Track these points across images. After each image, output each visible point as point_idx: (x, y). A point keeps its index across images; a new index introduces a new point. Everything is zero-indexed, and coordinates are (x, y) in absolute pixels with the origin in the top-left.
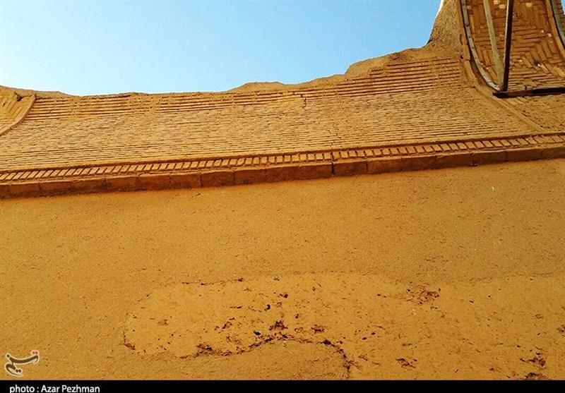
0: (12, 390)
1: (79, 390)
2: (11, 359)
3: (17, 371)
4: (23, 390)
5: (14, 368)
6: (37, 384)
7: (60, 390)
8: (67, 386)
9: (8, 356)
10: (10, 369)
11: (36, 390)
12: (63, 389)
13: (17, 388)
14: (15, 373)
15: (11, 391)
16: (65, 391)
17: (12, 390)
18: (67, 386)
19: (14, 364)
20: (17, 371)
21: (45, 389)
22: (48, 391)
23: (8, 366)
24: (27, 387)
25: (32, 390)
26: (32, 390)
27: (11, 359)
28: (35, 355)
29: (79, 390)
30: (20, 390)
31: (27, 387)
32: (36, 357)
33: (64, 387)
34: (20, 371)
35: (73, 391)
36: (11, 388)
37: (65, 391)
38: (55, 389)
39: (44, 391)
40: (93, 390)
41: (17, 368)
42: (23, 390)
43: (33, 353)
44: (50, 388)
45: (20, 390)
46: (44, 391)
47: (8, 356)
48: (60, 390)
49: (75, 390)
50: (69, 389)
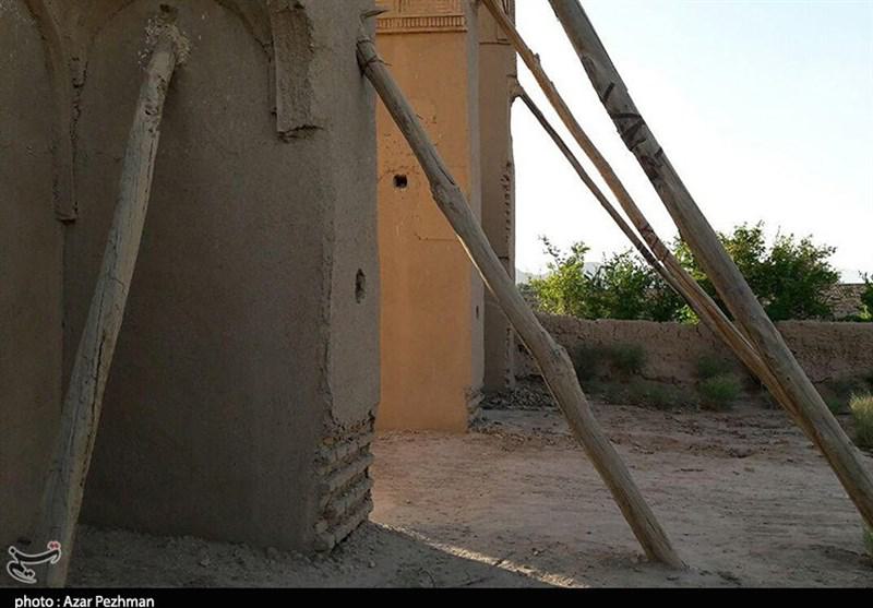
0: (19, 603)
1: (122, 603)
2: (17, 555)
3: (26, 574)
4: (36, 603)
5: (22, 570)
6: (58, 594)
7: (93, 603)
8: (104, 598)
9: (13, 551)
10: (14, 570)
11: (56, 603)
12: (97, 602)
13: (26, 600)
14: (24, 577)
15: (17, 605)
16: (101, 604)
17: (19, 603)
18: (104, 598)
19: (22, 563)
20: (26, 574)
21: (70, 603)
22: (75, 605)
23: (13, 566)
24: (42, 599)
25: (49, 603)
26: (49, 603)
27: (17, 555)
28: (55, 549)
29: (122, 603)
30: (32, 603)
31: (42, 599)
32: (56, 552)
33: (99, 599)
34: (31, 574)
35: (113, 605)
36: (17, 601)
37: (101, 604)
38: (85, 602)
39: (68, 605)
40: (143, 603)
41: (25, 570)
42: (36, 603)
43: (52, 546)
44: (78, 600)
45: (32, 603)
46: (68, 605)
47: (13, 551)
48: (93, 603)
49: (117, 603)
50: (106, 602)
